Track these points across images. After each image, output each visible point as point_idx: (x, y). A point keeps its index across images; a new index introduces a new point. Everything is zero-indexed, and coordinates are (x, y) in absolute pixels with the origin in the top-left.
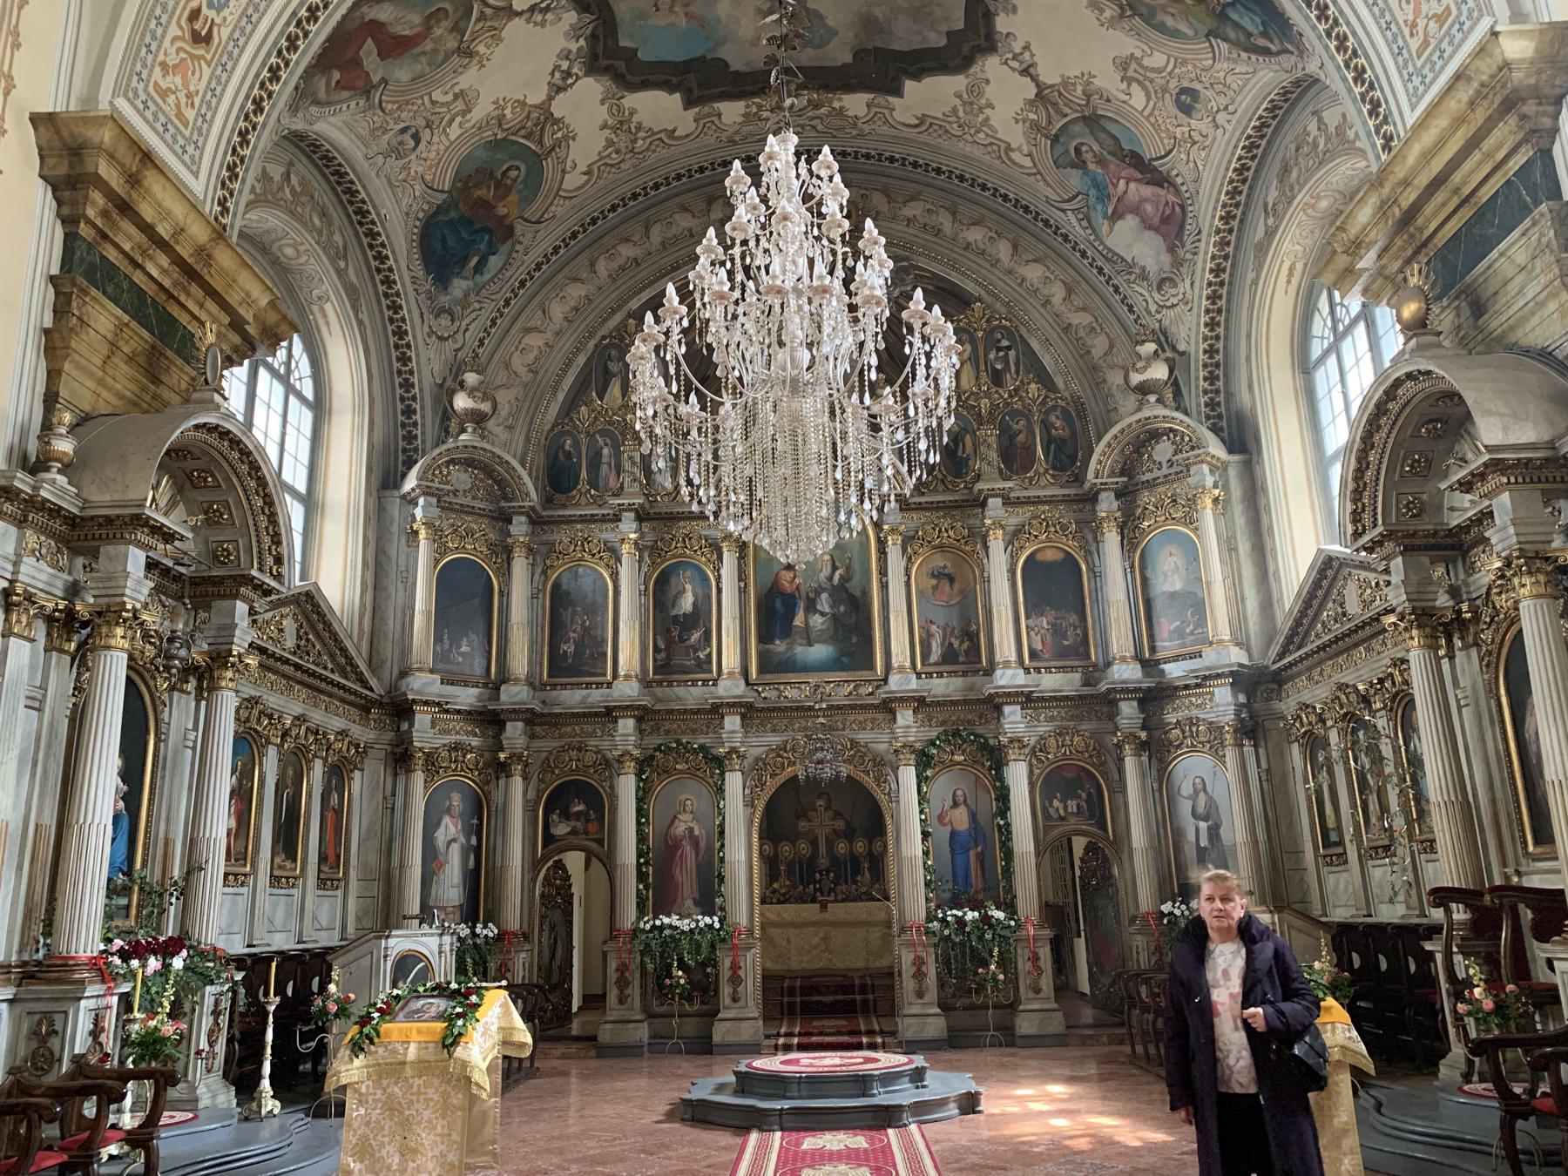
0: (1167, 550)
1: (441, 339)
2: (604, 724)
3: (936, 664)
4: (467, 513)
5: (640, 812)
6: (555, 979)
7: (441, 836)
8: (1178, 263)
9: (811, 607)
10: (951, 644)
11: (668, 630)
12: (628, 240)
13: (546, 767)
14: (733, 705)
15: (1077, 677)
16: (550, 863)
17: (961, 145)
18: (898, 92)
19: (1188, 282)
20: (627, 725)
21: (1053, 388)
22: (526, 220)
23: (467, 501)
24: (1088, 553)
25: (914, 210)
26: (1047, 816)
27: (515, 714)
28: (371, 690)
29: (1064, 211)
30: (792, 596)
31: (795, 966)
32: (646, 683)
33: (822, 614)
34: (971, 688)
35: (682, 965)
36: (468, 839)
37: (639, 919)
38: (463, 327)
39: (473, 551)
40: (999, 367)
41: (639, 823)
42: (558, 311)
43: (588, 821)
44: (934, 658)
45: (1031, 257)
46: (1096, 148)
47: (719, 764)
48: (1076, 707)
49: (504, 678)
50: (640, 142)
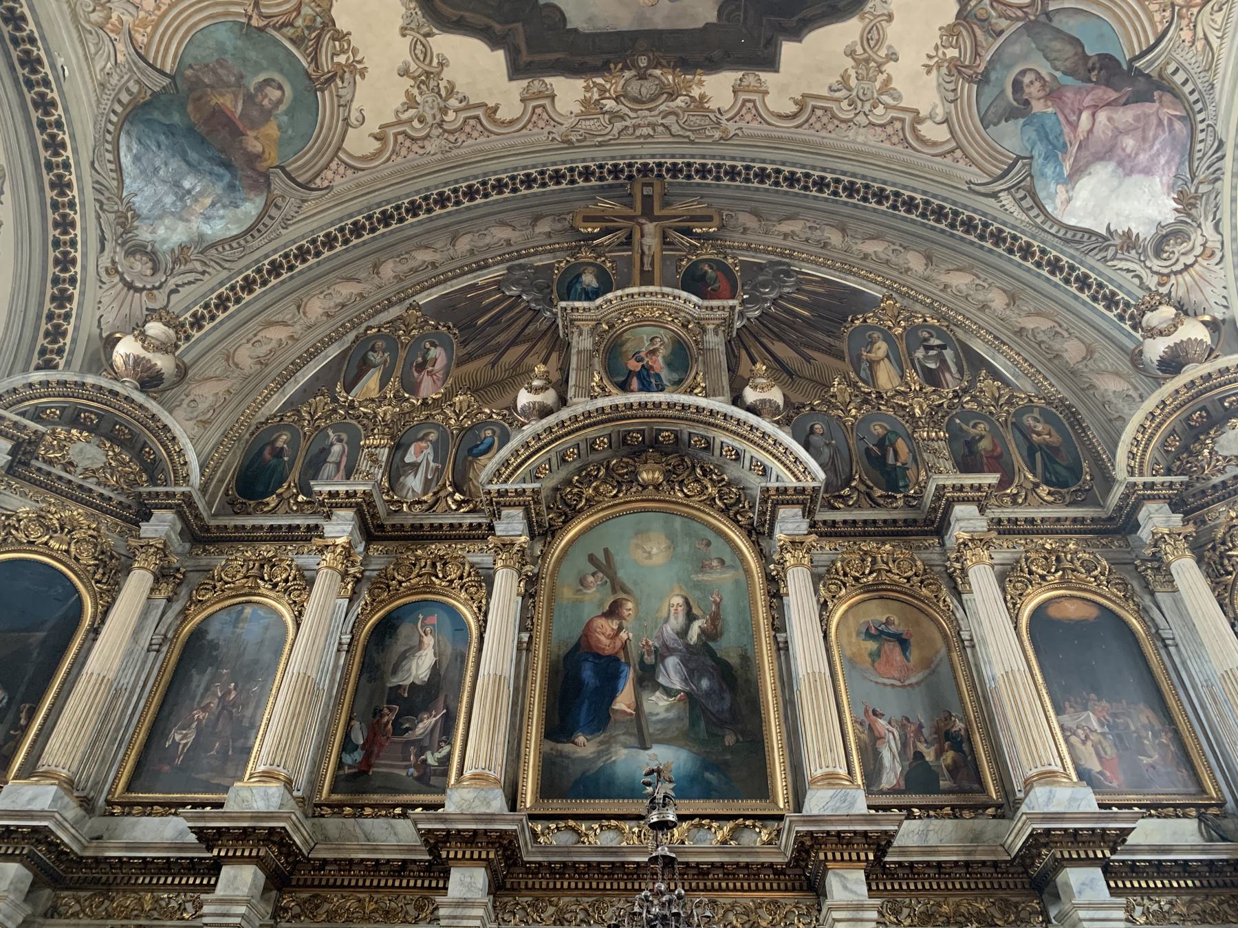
1: (130, 286)
3: (893, 791)
10: (919, 756)
14: (471, 839)
17: (851, 134)
18: (770, 63)
19: (1208, 227)
29: (994, 195)
34: (976, 837)
40: (933, 366)
45: (951, 267)
46: (1045, 70)
50: (451, 115)
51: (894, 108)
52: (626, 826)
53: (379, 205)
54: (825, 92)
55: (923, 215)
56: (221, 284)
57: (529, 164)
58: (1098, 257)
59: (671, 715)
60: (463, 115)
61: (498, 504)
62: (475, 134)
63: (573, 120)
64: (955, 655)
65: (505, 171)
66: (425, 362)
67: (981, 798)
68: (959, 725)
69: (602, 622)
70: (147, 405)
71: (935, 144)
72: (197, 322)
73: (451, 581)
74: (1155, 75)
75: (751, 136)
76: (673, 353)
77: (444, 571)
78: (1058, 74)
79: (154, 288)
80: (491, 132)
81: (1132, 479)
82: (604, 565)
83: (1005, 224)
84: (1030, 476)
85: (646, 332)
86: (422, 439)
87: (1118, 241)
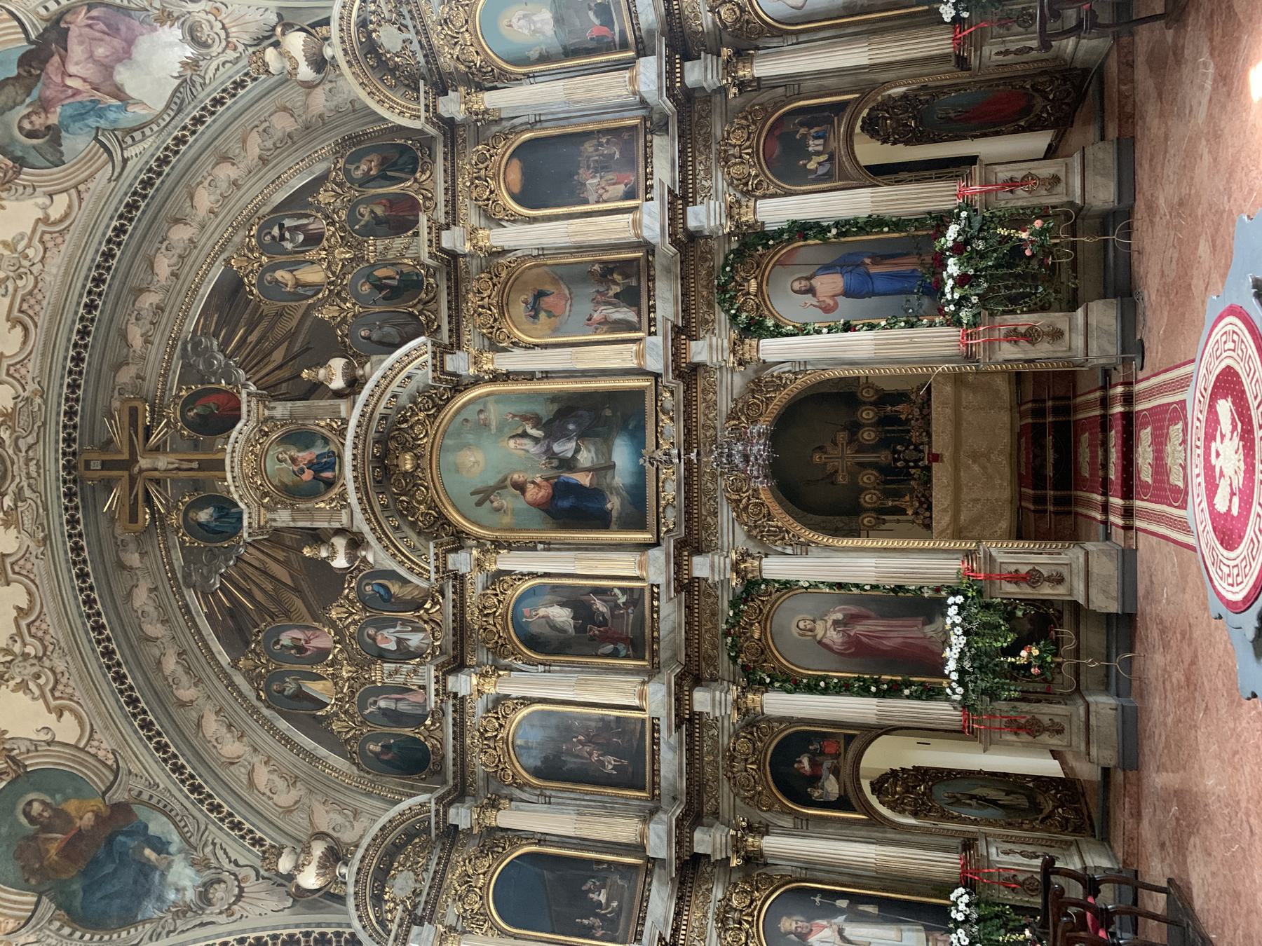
0: (504, 30)
1: (239, 897)
2: (702, 725)
4: (442, 881)
5: (812, 687)
6: (1024, 803)
8: (166, 17)
9: (568, 464)
11: (592, 639)
12: (159, 663)
13: (754, 800)
16: (874, 800)
17: (48, 278)
20: (702, 700)
21: (328, 172)
22: (109, 789)
23: (428, 876)
24: (514, 130)
25: (136, 335)
27: (682, 836)
29: (125, 161)
30: (555, 487)
31: (1007, 494)
32: (653, 671)
33: (577, 451)
34: (668, 270)
35: (1013, 650)
36: (841, 911)
37: (947, 699)
38: (232, 867)
39: (489, 871)
40: (301, 238)
41: (825, 692)
42: (231, 747)
43: (822, 753)
44: (631, 315)
45: (188, 204)
46: (23, 110)
47: (752, 587)
48: (694, 141)
49: (638, 848)
50: (29, 650)
51: (31, 239)
52: (662, 477)
53: (121, 708)
54: (7, 300)
55: (131, 220)
56: (221, 829)
57: (67, 576)
58: (200, 89)
59: (593, 449)
60: (28, 639)
61: (442, 570)
62: (44, 626)
63: (24, 536)
64: (549, 262)
65: (76, 598)
66: (295, 647)
67: (642, 262)
68: (596, 267)
69: (528, 495)
70: (365, 846)
71: (70, 207)
72: (258, 842)
73: (499, 601)
74: (45, 25)
75: (41, 370)
76: (294, 444)
77: (490, 608)
78: (28, 100)
79: (237, 879)
80: (41, 612)
81: (423, 119)
82: (484, 495)
83: (153, 155)
84: (409, 184)
86: (374, 639)
87: (189, 73)
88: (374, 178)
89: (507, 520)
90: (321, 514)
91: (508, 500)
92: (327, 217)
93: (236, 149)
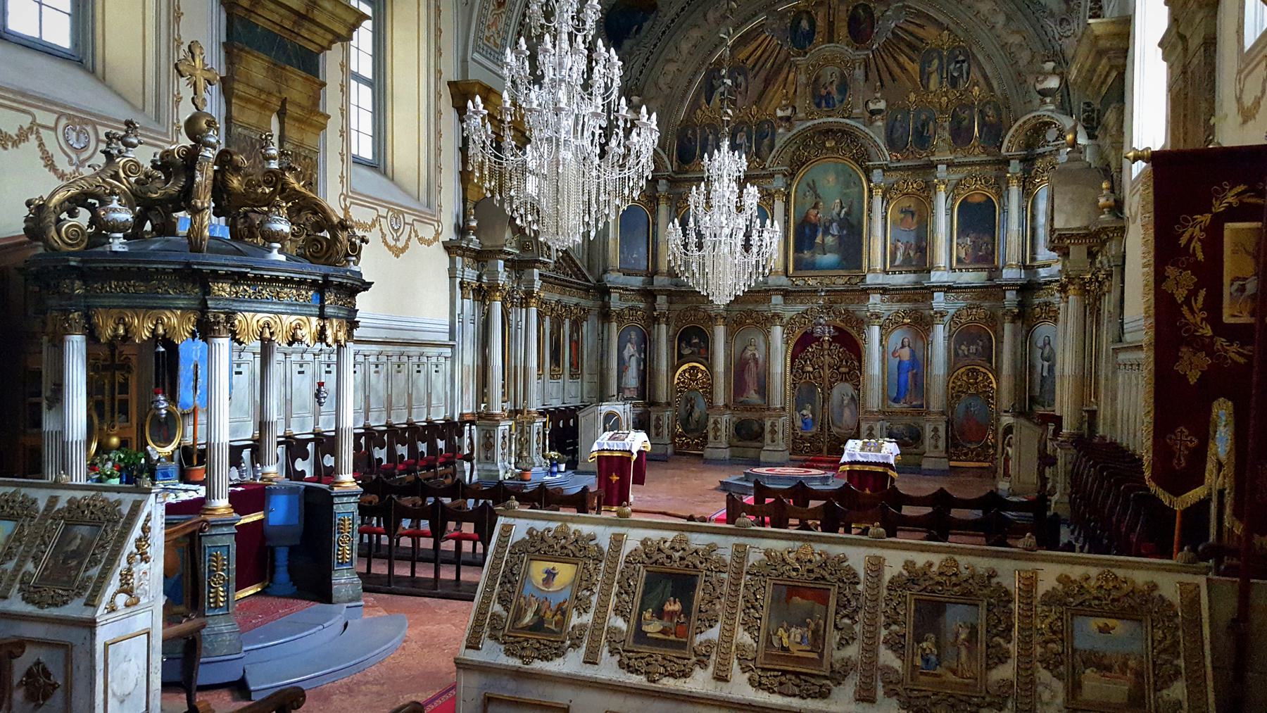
7: (626, 354)
13: (678, 319)
15: (984, 274)
26: (957, 354)
27: (661, 292)
28: (590, 282)
40: (956, 74)
44: (897, 263)
82: (812, 187)
85: (829, 70)
88: (983, 119)
89: (800, 199)
90: (804, 103)
91: (810, 200)
92: (965, 90)
93: (1013, 26)
